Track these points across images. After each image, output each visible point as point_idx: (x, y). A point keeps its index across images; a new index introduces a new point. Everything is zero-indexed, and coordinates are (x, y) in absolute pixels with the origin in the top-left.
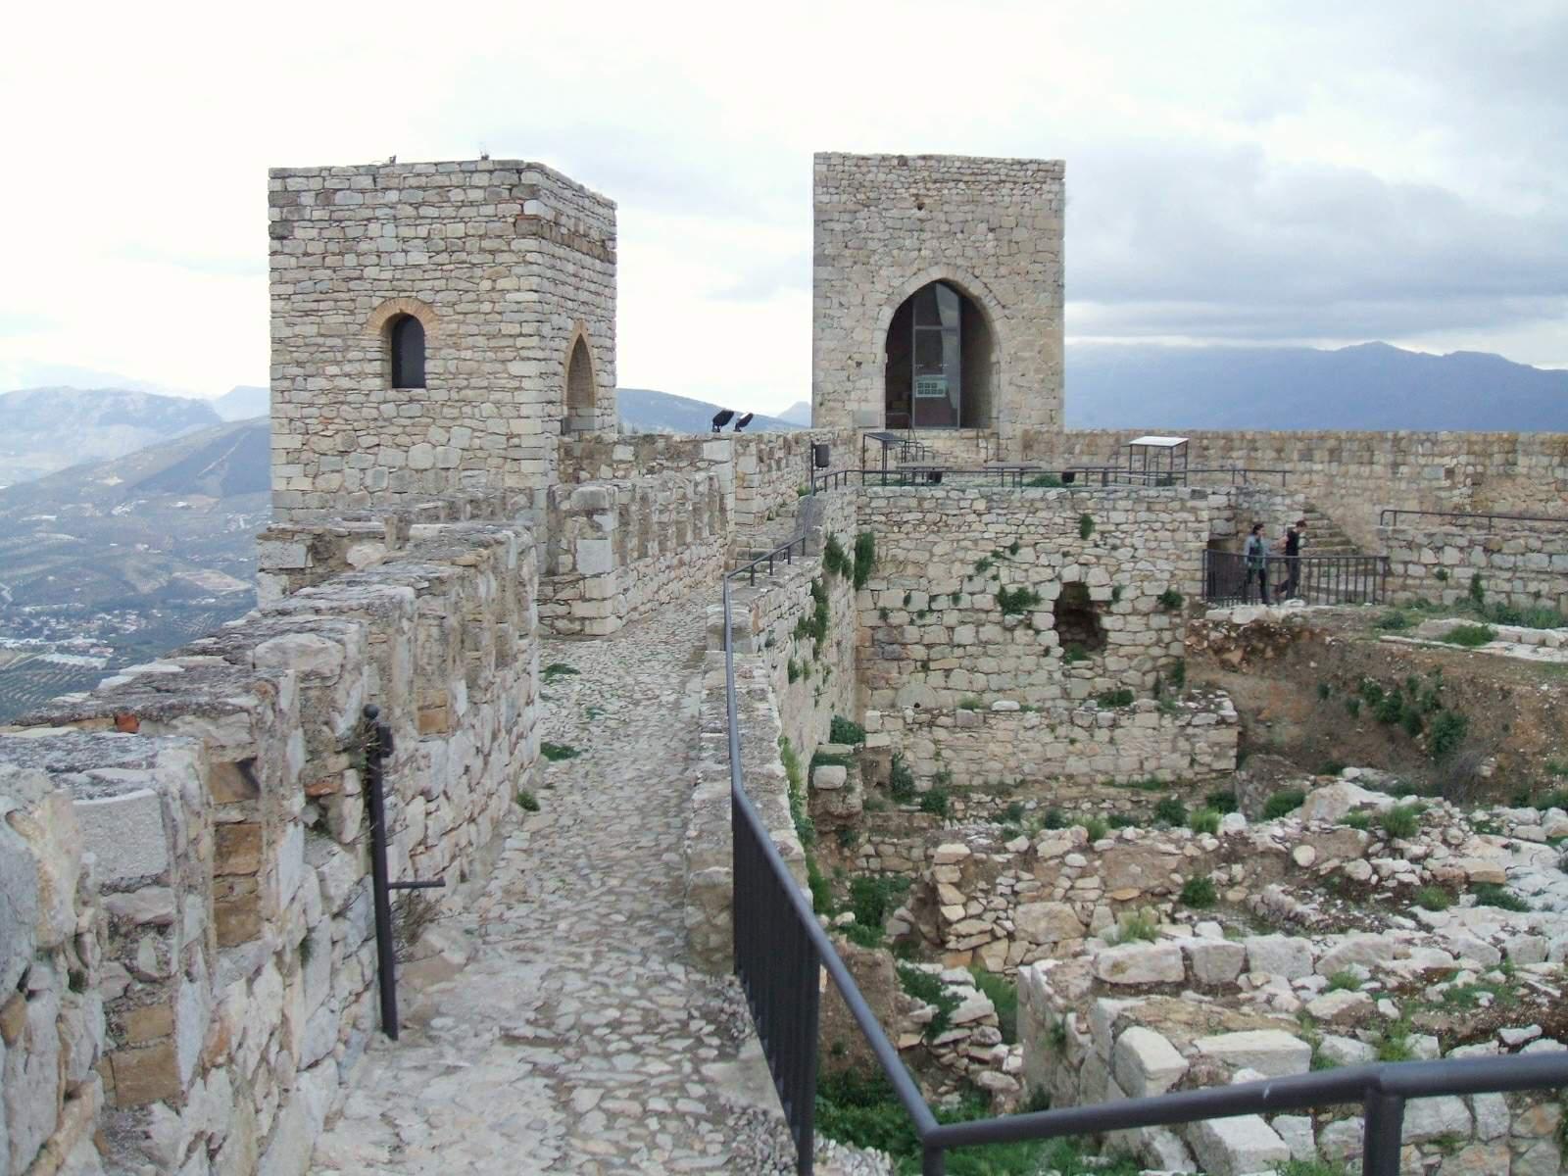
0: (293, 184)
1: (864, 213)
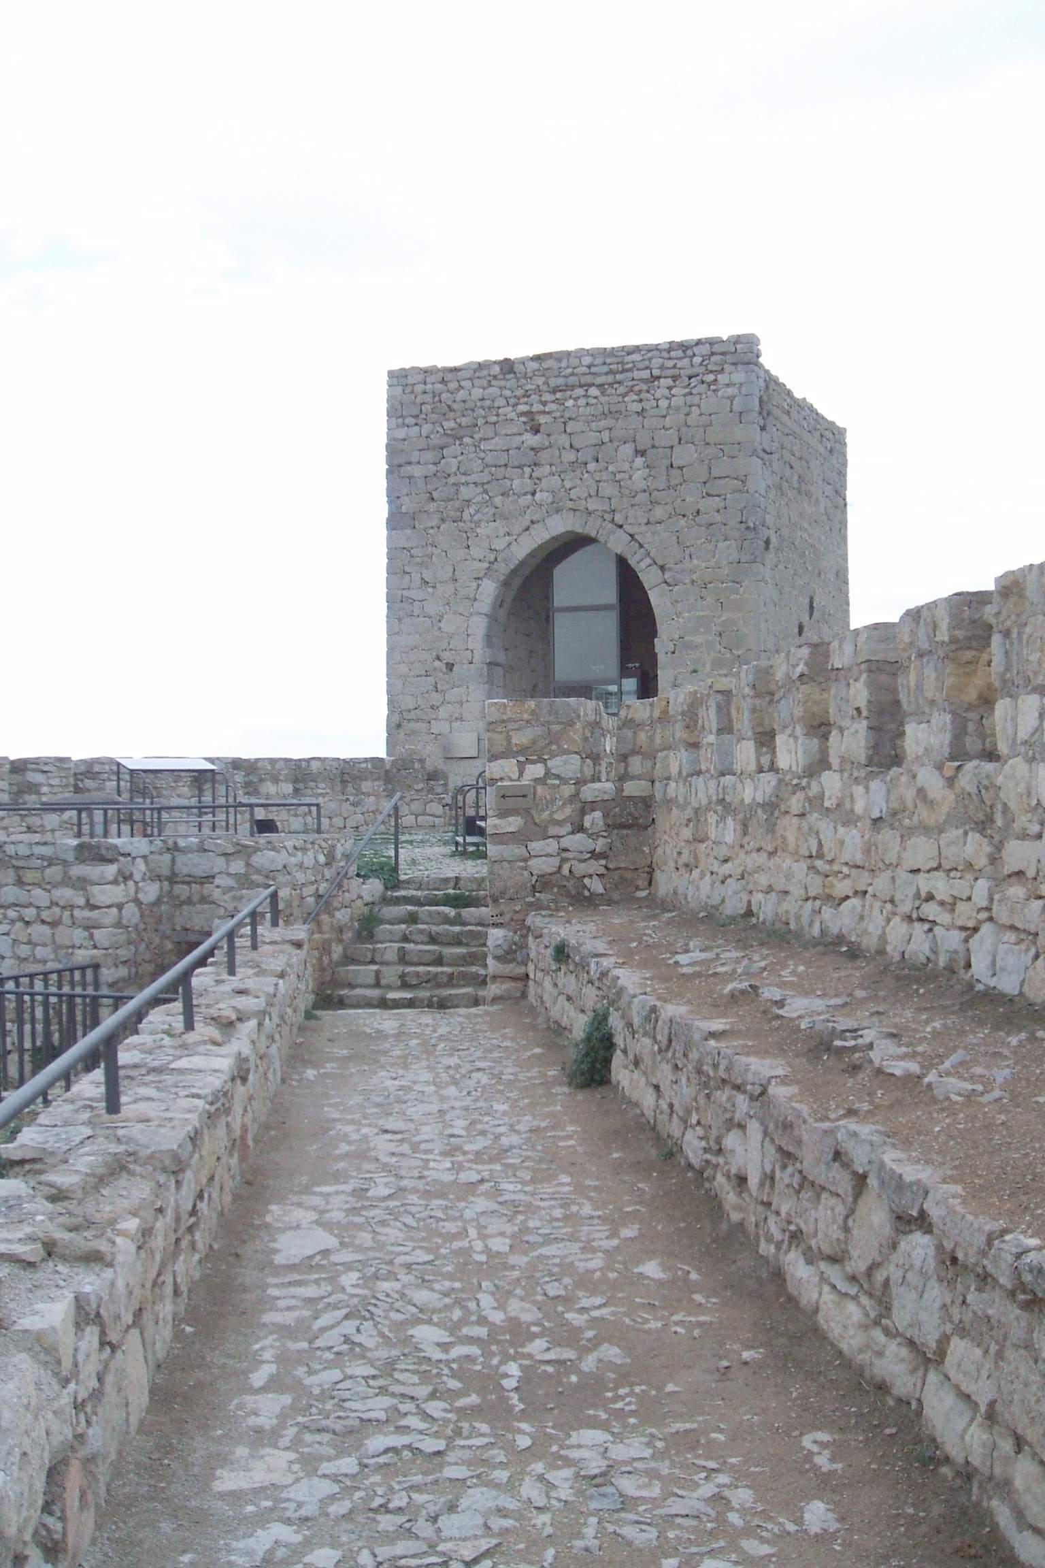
1: (456, 449)
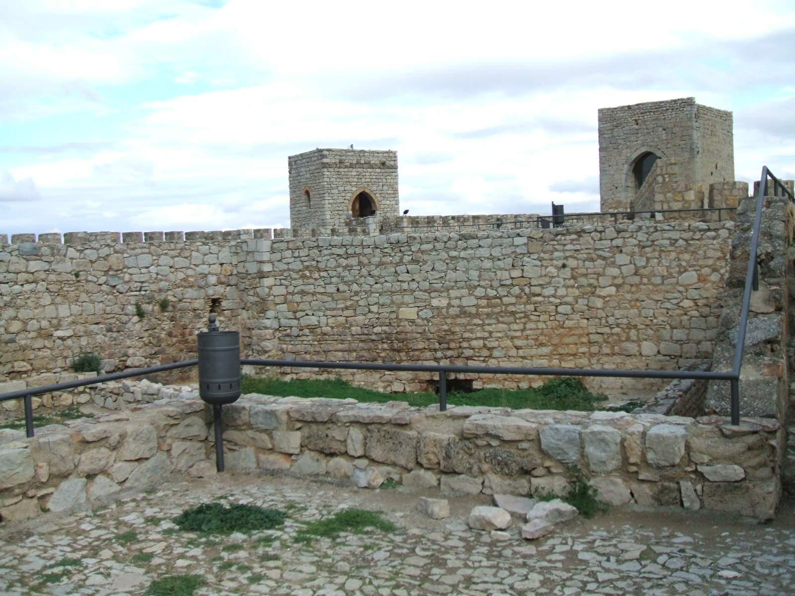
1: (616, 130)
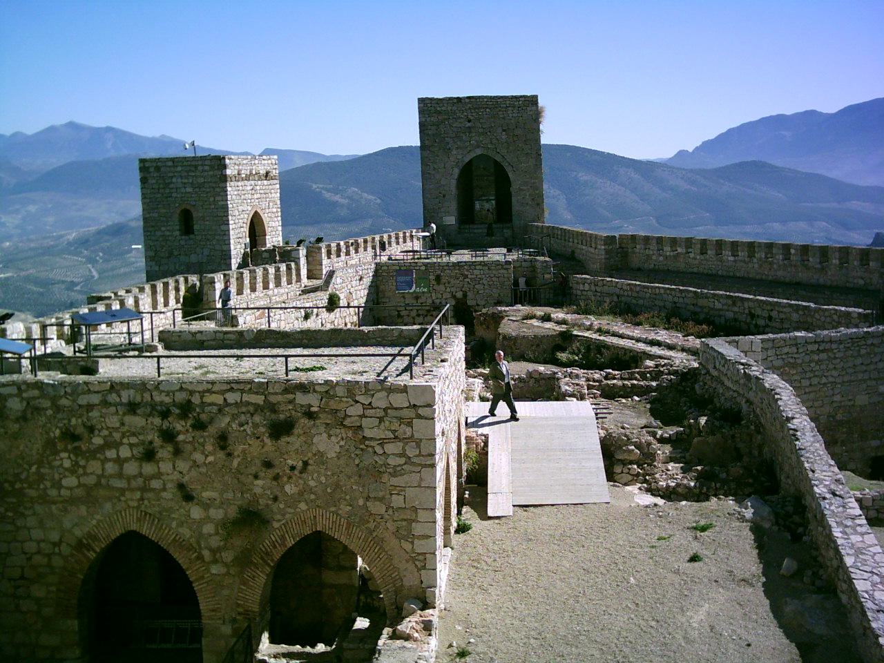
0: (147, 165)
